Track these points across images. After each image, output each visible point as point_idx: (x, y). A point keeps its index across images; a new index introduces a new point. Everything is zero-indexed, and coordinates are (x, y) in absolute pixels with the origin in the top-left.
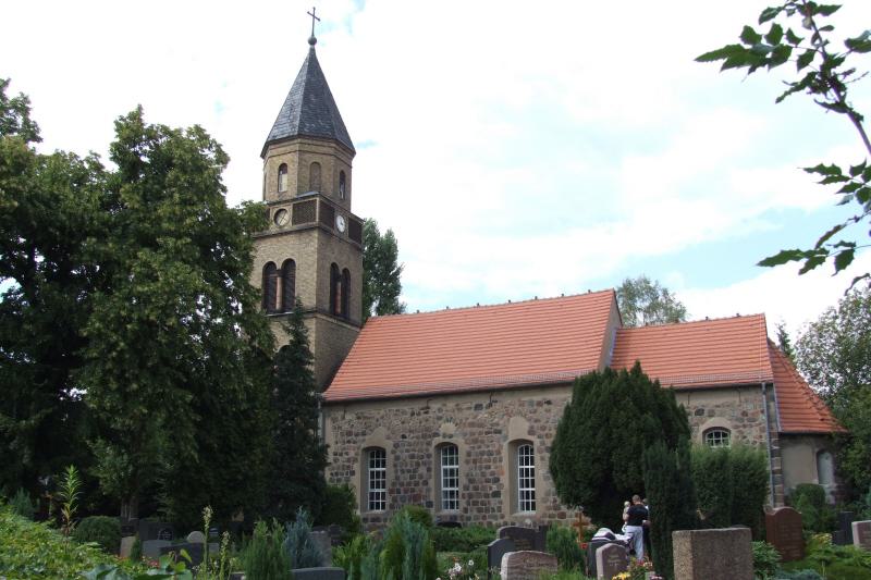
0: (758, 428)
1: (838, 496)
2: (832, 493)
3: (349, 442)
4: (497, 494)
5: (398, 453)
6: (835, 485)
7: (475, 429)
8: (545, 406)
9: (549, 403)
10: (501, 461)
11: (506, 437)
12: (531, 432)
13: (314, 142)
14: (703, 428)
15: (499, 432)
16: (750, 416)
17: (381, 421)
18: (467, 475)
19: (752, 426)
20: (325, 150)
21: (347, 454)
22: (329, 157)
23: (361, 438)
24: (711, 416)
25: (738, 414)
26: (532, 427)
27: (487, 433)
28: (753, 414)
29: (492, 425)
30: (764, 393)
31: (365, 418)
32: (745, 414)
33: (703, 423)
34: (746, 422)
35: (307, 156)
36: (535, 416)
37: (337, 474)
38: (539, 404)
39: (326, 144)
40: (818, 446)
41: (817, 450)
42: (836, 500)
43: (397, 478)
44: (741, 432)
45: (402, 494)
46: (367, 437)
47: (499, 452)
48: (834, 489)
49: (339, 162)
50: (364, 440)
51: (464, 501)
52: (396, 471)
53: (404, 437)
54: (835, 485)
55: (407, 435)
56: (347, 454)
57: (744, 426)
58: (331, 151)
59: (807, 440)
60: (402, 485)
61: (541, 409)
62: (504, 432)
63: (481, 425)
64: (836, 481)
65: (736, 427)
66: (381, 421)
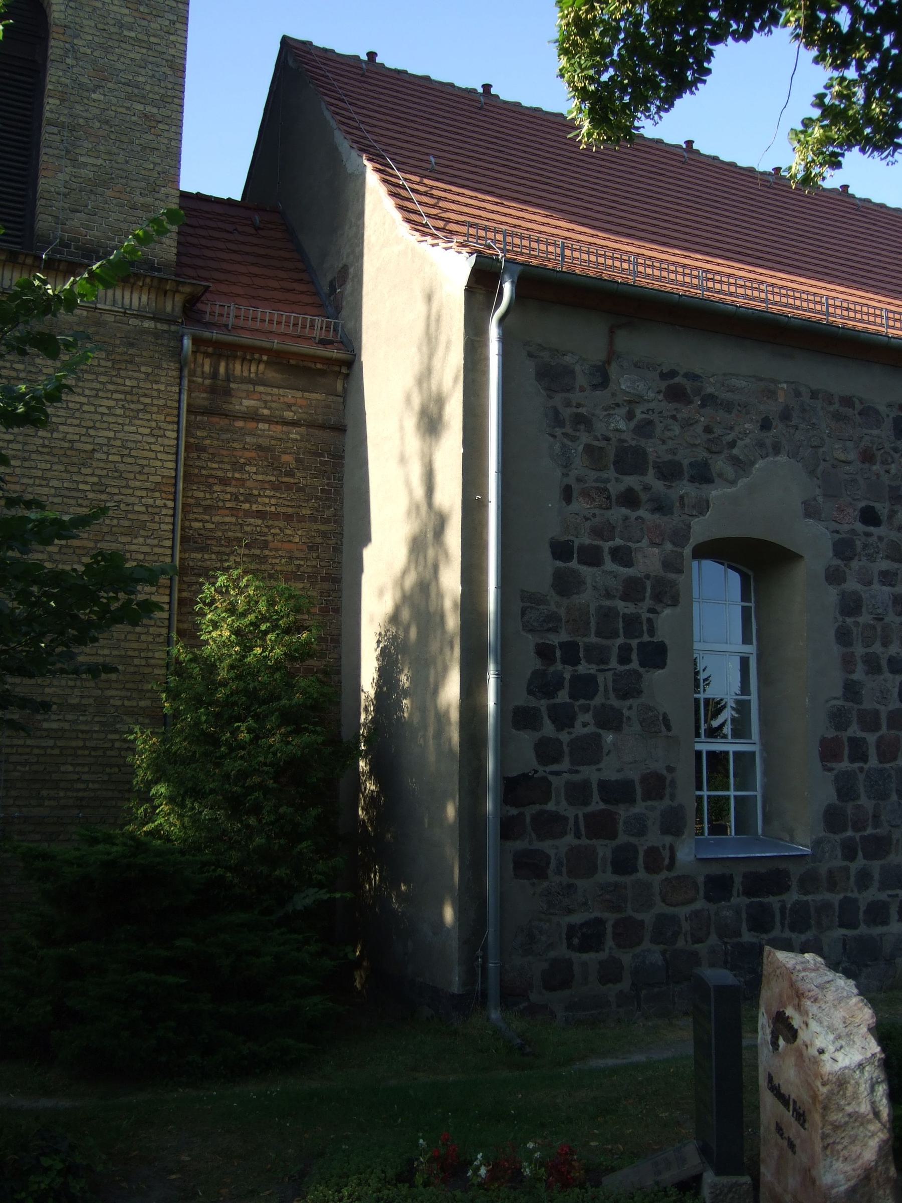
3: (630, 499)
5: (852, 585)
17: (778, 428)
21: (622, 556)
23: (685, 488)
31: (709, 400)
37: (571, 653)
43: (852, 690)
45: (873, 762)
46: (715, 493)
50: (703, 507)
52: (848, 663)
53: (870, 517)
55: (882, 508)
56: (622, 556)
60: (870, 721)
66: (778, 428)
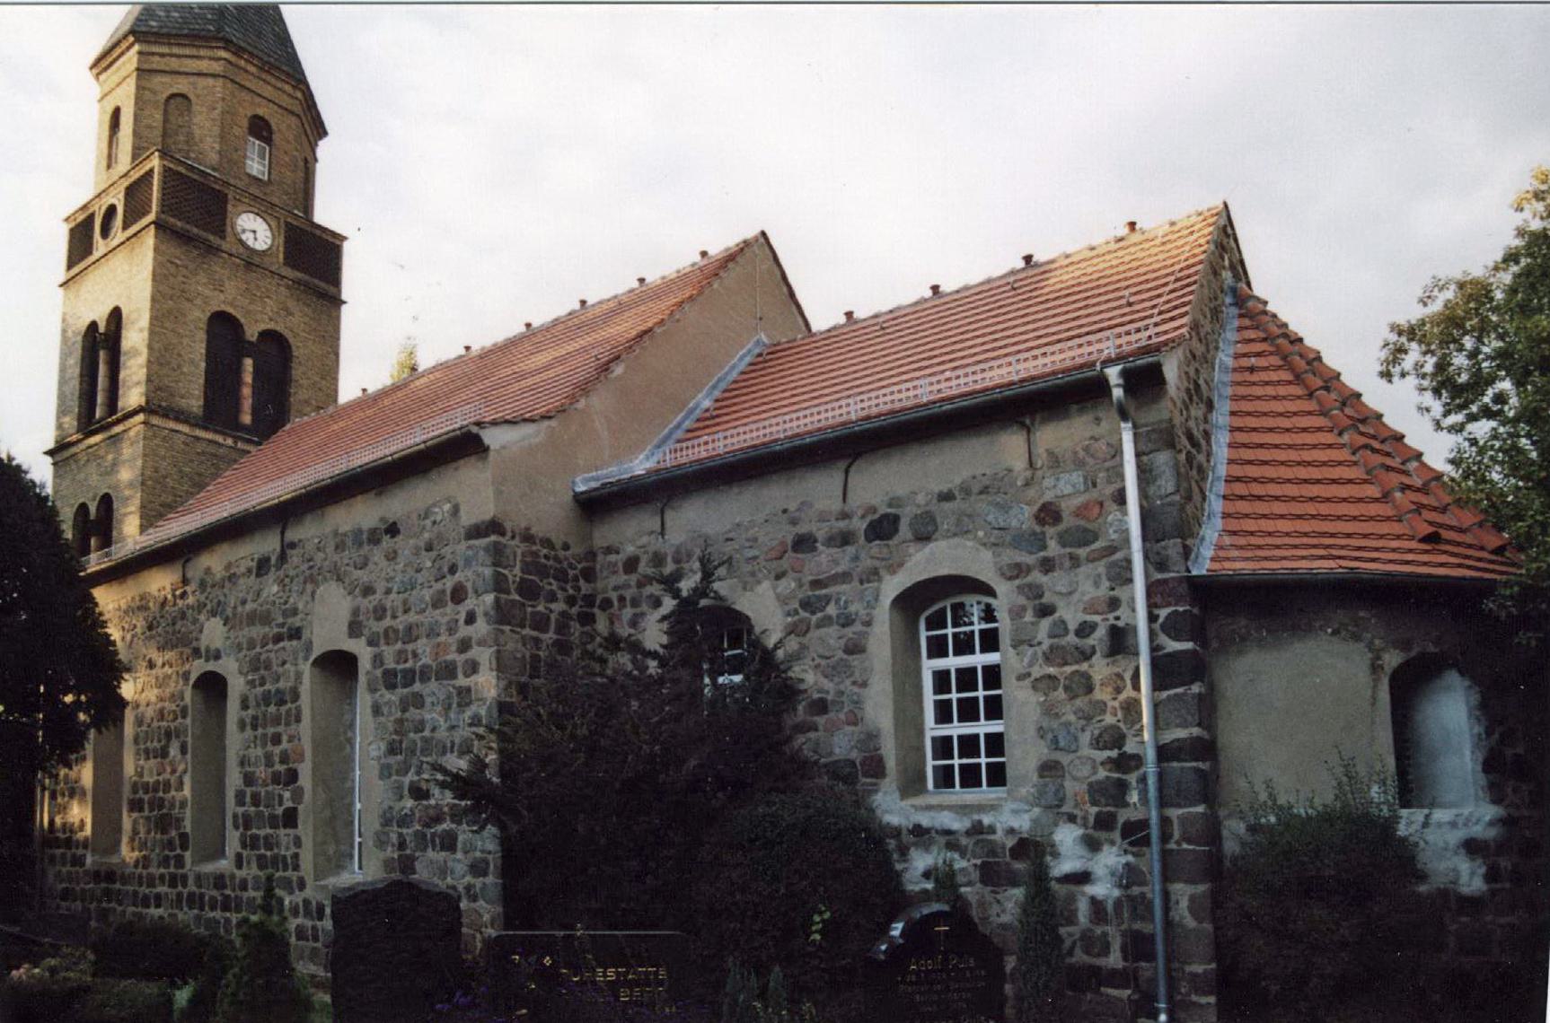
0: (1101, 567)
1: (1505, 863)
2: (1472, 847)
4: (290, 818)
6: (1490, 812)
7: (257, 631)
8: (387, 542)
9: (393, 530)
10: (298, 720)
11: (309, 648)
12: (355, 629)
13: (176, 50)
14: (893, 586)
15: (296, 634)
16: (1068, 521)
18: (242, 764)
19: (1075, 561)
20: (203, 65)
22: (210, 81)
24: (923, 538)
25: (1022, 517)
26: (356, 612)
27: (278, 639)
28: (1080, 512)
29: (285, 614)
30: (1124, 415)
32: (1048, 514)
33: (893, 569)
34: (1053, 549)
35: (158, 80)
36: (363, 576)
38: (374, 538)
39: (202, 52)
40: (1405, 645)
41: (1392, 659)
42: (1492, 876)
44: (1035, 592)
47: (296, 696)
48: (1478, 831)
49: (245, 95)
51: (237, 834)
54: (1490, 812)
57: (1048, 566)
58: (217, 67)
59: (1341, 616)
61: (377, 555)
62: (306, 634)
63: (266, 619)
64: (1496, 793)
65: (1017, 571)
